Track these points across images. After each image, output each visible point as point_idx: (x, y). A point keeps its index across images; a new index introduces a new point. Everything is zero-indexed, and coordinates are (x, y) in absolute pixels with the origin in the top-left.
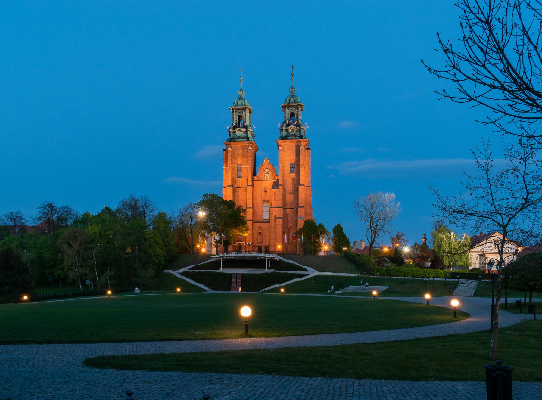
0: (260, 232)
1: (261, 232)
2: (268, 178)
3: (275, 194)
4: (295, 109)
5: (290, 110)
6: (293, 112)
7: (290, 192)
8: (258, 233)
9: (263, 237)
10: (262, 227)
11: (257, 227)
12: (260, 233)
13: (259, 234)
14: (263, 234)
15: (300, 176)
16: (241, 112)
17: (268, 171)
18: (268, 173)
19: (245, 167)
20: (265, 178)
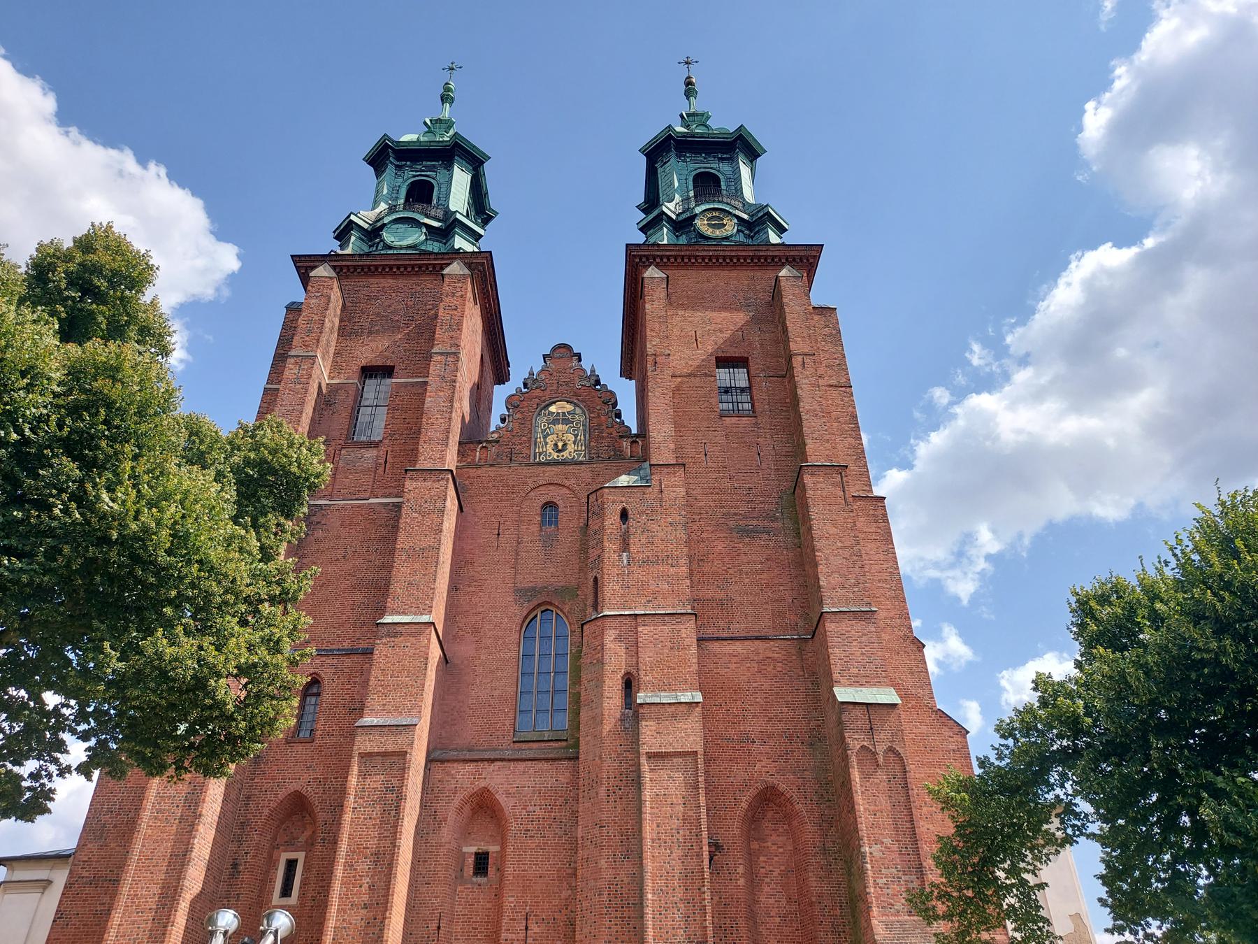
0: (484, 848)
1: (493, 849)
2: (571, 447)
3: (624, 515)
4: (722, 159)
5: (692, 166)
6: (707, 170)
7: (732, 524)
8: (463, 856)
9: (510, 900)
10: (501, 798)
11: (456, 802)
12: (481, 863)
13: (469, 870)
14: (509, 870)
15: (804, 416)
16: (433, 169)
17: (569, 407)
18: (566, 422)
19: (413, 384)
20: (550, 448)
